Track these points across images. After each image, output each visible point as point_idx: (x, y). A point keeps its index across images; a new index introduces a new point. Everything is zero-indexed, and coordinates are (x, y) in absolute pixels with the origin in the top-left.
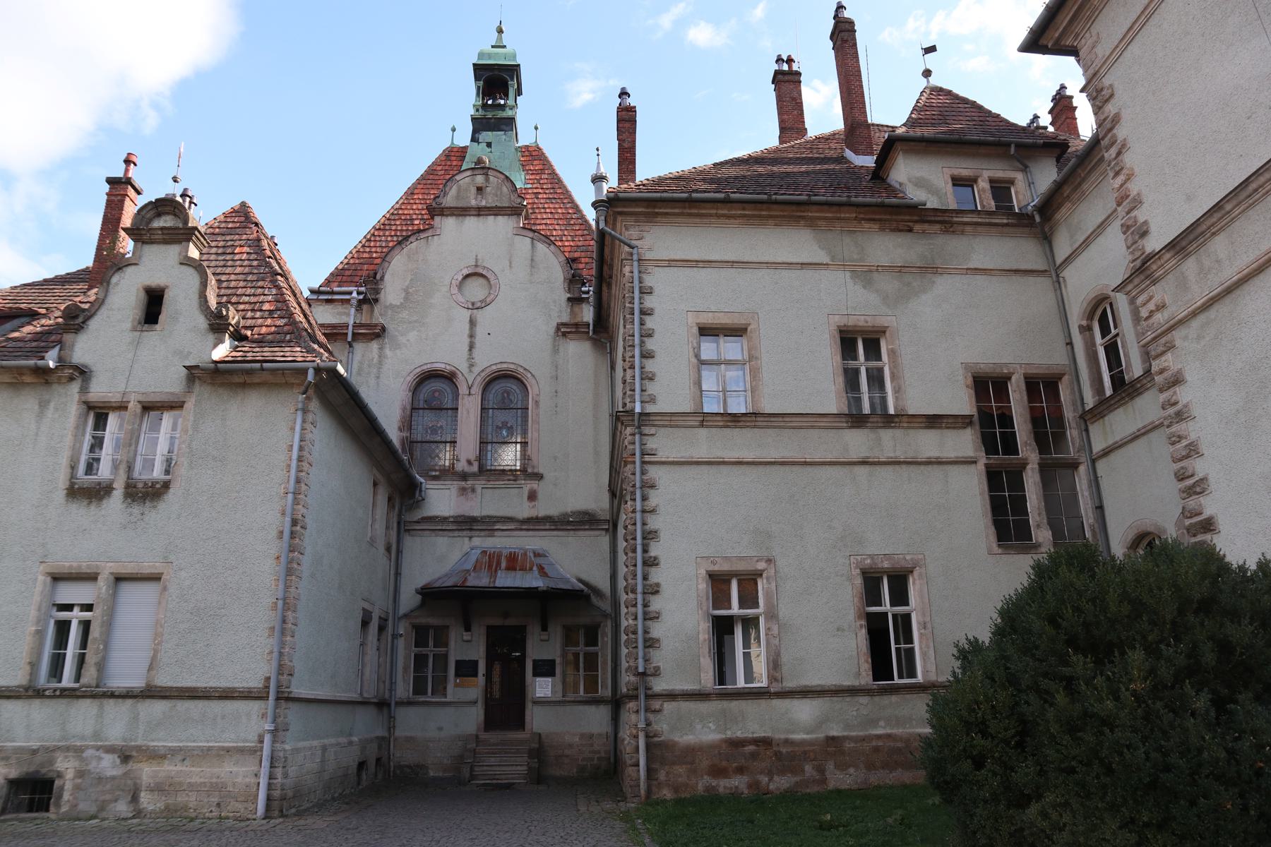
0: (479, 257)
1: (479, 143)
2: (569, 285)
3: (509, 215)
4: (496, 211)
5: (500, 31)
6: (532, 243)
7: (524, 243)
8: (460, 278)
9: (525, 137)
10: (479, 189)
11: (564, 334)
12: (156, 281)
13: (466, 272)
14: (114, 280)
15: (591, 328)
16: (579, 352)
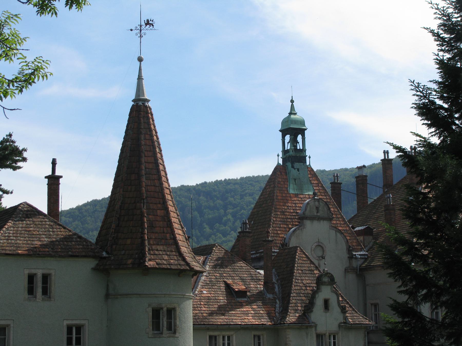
0: (319, 238)
1: (295, 169)
2: (348, 252)
3: (328, 220)
4: (323, 219)
5: (292, 101)
6: (336, 233)
7: (333, 232)
8: (314, 247)
9: (308, 164)
10: (317, 207)
11: (348, 272)
12: (327, 297)
13: (316, 244)
14: (317, 296)
15: (358, 270)
16: (352, 277)
